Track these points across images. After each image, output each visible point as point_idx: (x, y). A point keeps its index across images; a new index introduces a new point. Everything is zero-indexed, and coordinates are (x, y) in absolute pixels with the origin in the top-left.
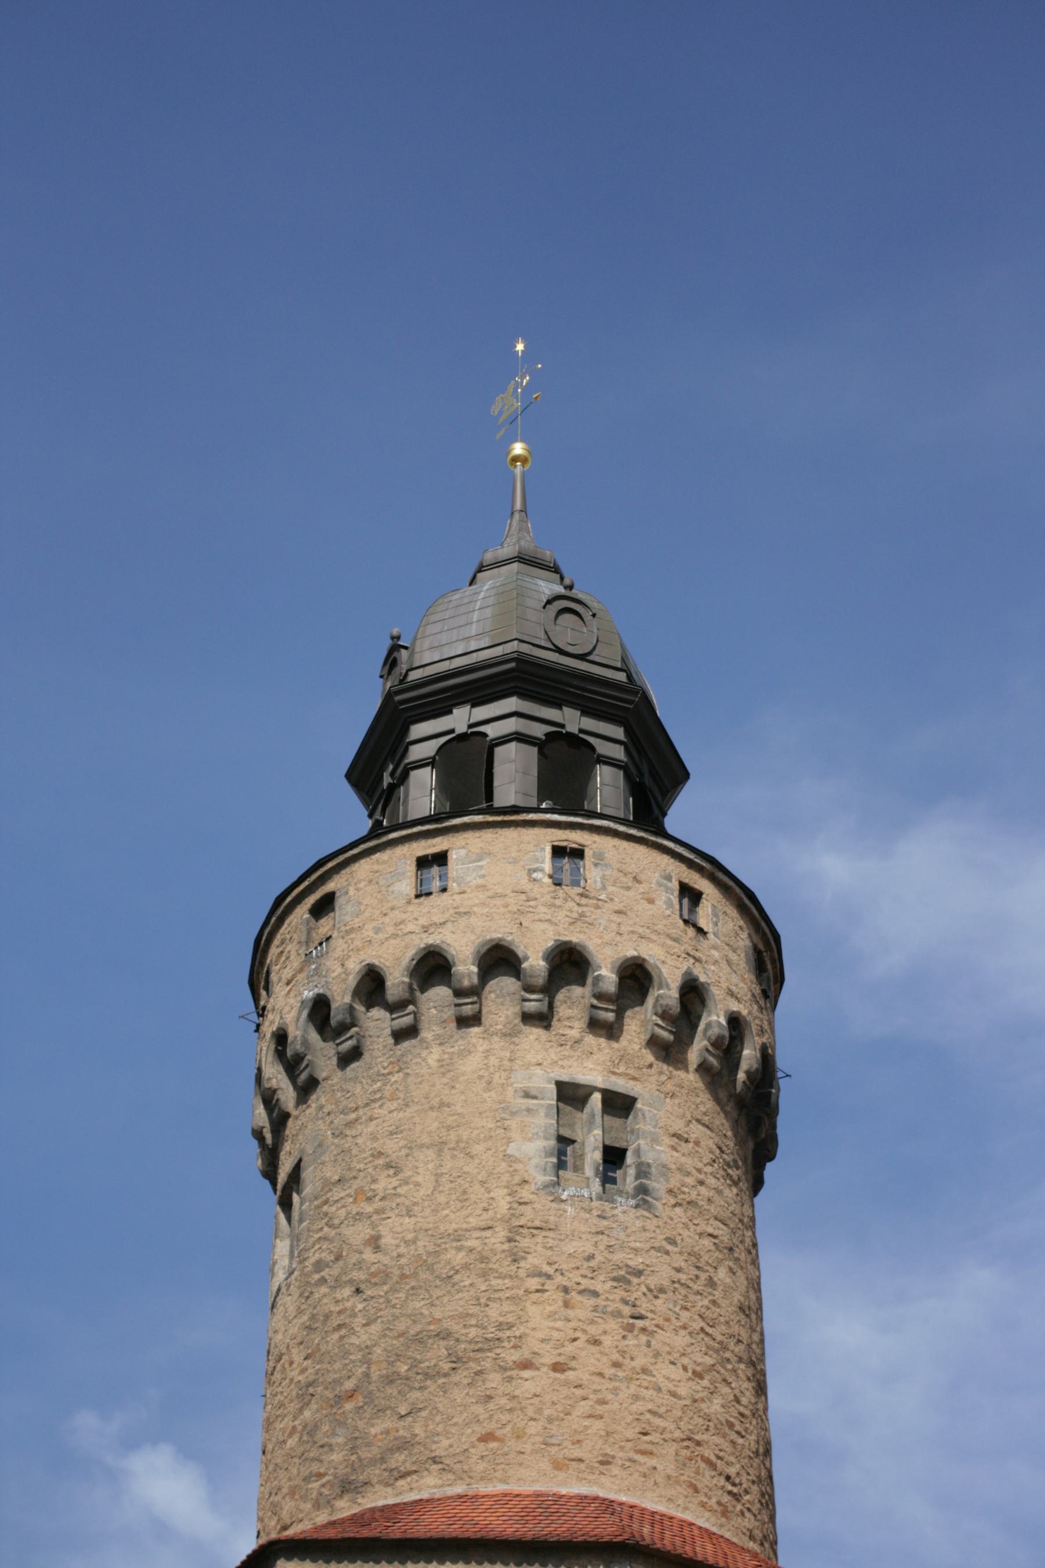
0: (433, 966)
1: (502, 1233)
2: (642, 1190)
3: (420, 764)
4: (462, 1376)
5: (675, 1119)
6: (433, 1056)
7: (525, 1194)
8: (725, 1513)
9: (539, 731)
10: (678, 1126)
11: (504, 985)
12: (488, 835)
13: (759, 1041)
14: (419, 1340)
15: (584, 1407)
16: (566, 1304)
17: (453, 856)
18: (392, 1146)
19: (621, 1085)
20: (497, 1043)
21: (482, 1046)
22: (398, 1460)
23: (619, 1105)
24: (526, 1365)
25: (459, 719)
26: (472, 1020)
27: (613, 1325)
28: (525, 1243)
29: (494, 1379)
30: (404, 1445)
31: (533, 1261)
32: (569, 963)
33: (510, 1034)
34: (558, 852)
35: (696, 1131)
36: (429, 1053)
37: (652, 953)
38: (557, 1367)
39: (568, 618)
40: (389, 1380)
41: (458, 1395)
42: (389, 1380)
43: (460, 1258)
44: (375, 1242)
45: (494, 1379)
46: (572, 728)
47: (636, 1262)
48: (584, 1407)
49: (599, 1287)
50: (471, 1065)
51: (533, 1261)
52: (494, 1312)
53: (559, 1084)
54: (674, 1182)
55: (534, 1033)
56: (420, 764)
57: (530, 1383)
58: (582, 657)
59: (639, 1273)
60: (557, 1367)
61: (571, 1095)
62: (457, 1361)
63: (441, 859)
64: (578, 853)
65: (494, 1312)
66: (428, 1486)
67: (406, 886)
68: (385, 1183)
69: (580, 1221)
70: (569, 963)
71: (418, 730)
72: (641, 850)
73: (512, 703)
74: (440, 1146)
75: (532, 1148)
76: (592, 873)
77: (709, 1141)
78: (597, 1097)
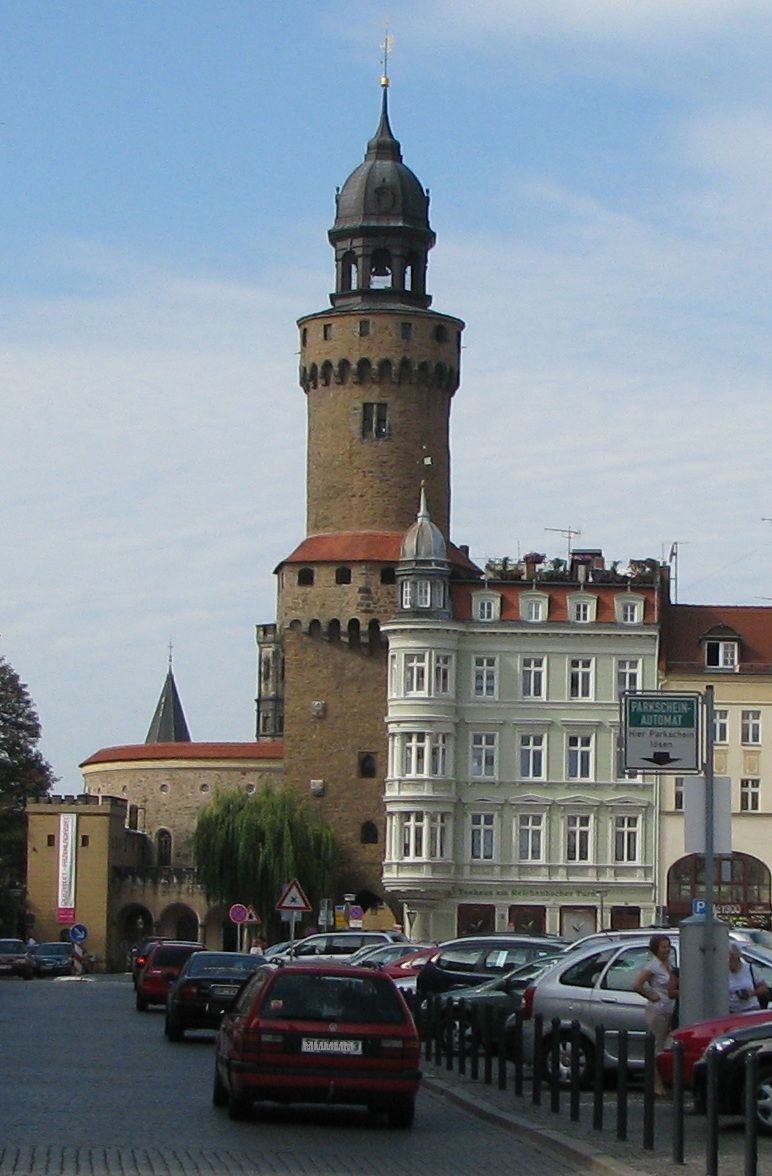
1: (347, 455)
4: (338, 499)
14: (329, 488)
15: (369, 506)
16: (365, 476)
17: (333, 326)
20: (347, 390)
21: (343, 392)
24: (353, 496)
28: (353, 458)
30: (326, 518)
32: (364, 363)
38: (361, 496)
47: (385, 459)
49: (373, 470)
57: (355, 501)
59: (385, 462)
74: (332, 426)
75: (356, 427)
76: (371, 331)
78: (375, 406)
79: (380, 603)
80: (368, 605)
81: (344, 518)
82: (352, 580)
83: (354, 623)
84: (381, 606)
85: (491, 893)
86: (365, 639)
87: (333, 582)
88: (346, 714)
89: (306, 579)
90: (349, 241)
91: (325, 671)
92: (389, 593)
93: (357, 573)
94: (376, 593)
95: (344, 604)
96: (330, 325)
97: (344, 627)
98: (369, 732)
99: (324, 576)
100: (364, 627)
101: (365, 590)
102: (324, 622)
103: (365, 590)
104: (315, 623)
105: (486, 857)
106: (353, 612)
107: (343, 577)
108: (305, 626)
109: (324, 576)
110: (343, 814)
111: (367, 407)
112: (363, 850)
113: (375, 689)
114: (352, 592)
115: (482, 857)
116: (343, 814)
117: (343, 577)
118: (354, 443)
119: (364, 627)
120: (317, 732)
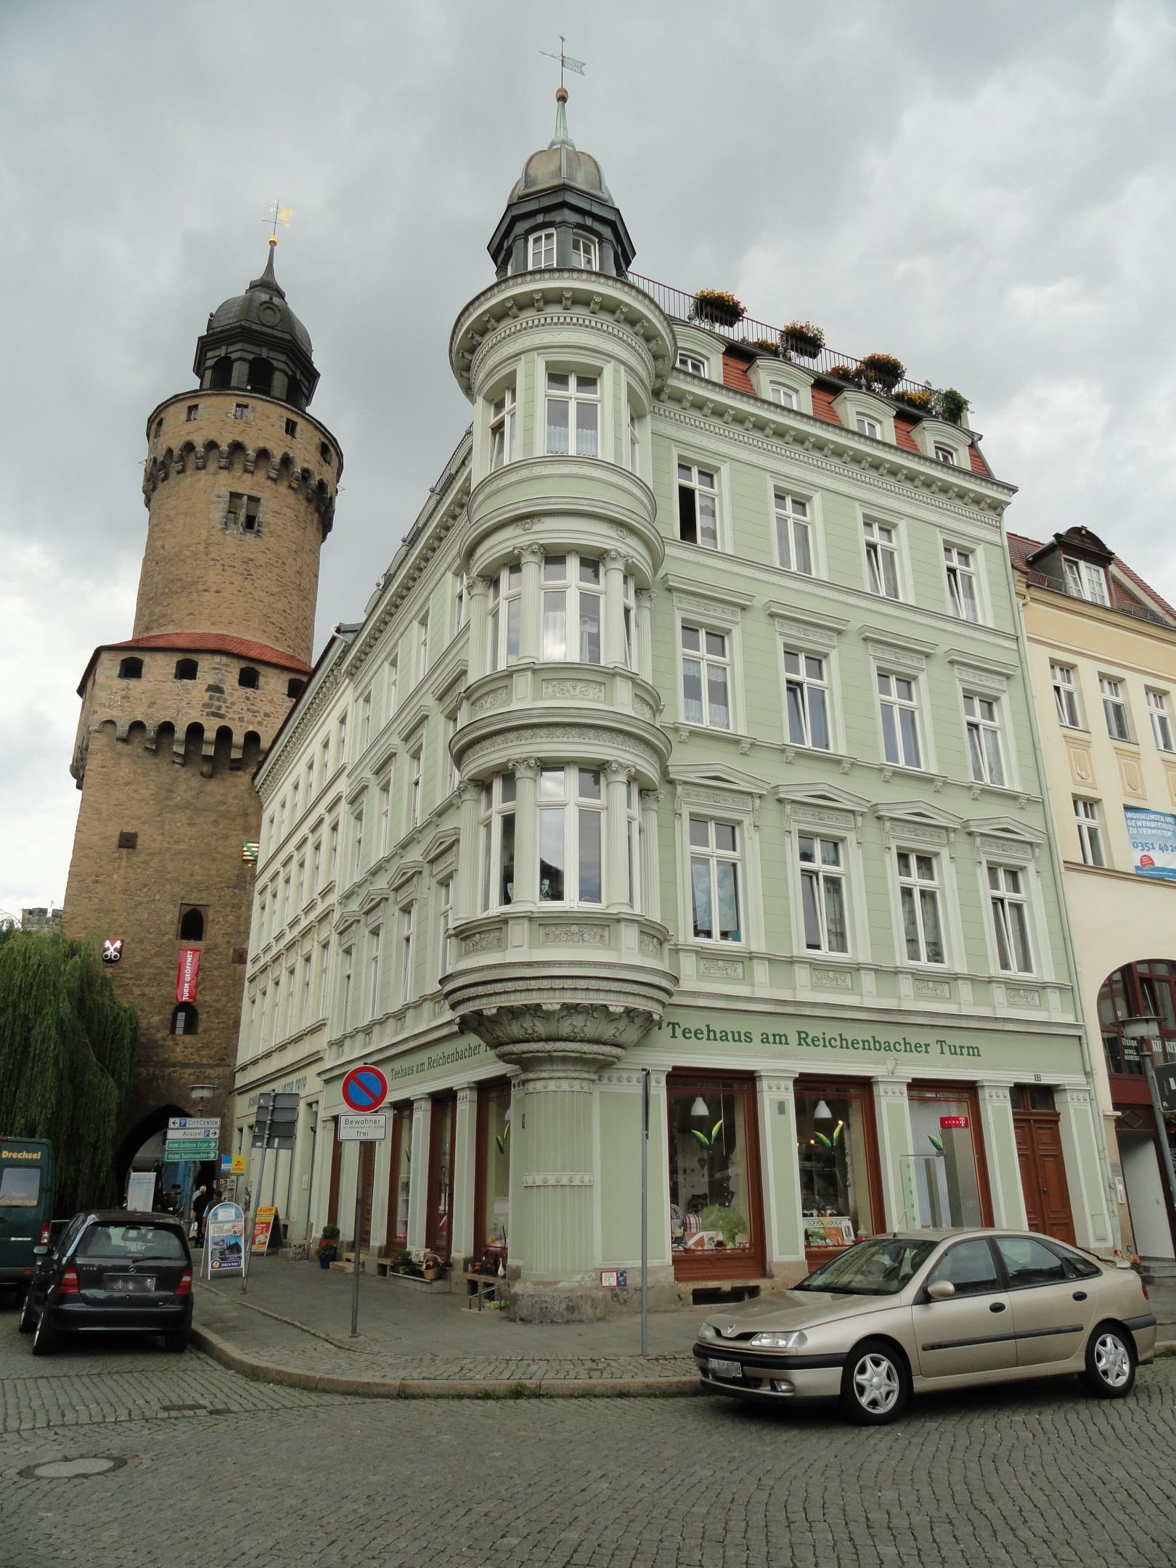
0: (189, 447)
2: (259, 531)
3: (208, 368)
4: (184, 594)
5: (279, 506)
6: (188, 481)
7: (213, 532)
8: (277, 639)
9: (251, 357)
10: (277, 508)
11: (214, 453)
12: (213, 399)
13: (317, 478)
14: (172, 581)
15: (225, 605)
18: (172, 513)
19: (254, 493)
20: (210, 477)
22: (162, 621)
23: (254, 500)
24: (206, 591)
25: (222, 352)
26: (204, 468)
27: (240, 577)
29: (195, 595)
30: (164, 616)
31: (213, 555)
32: (237, 447)
33: (215, 474)
34: (238, 405)
35: (285, 510)
36: (187, 479)
37: (270, 446)
38: (217, 592)
39: (269, 311)
40: (163, 594)
41: (182, 600)
42: (163, 594)
43: (188, 553)
44: (163, 547)
45: (195, 595)
46: (264, 356)
48: (225, 605)
50: (199, 485)
51: (213, 555)
52: (197, 573)
53: (231, 493)
54: (272, 528)
55: (225, 472)
56: (208, 368)
58: (272, 327)
60: (217, 592)
61: (235, 496)
62: (184, 588)
63: (196, 407)
64: (246, 406)
65: (197, 573)
66: (170, 629)
67: (184, 417)
68: (168, 526)
69: (234, 542)
70: (237, 447)
71: (210, 354)
72: (272, 406)
73: (239, 346)
74: (186, 514)
77: (290, 514)
78: (245, 498)
79: (235, 708)
80: (219, 708)
81: (191, 614)
82: (199, 674)
83: (195, 731)
84: (235, 712)
85: (749, 1039)
86: (209, 750)
87: (171, 677)
88: (167, 849)
89: (131, 669)
90: (224, 348)
91: (143, 791)
92: (248, 699)
93: (206, 665)
94: (231, 695)
95: (184, 704)
96: (196, 407)
97: (180, 733)
98: (199, 878)
99: (159, 668)
100: (210, 734)
101: (215, 689)
102: (151, 726)
103: (215, 689)
104: (137, 726)
105: (725, 935)
106: (195, 716)
107: (187, 671)
108: (123, 728)
109: (159, 668)
110: (147, 990)
111: (235, 496)
112: (171, 1043)
113: (215, 822)
114: (197, 689)
115: (716, 933)
116: (147, 990)
117: (187, 671)
118: (213, 532)
119: (210, 734)
120: (122, 872)
